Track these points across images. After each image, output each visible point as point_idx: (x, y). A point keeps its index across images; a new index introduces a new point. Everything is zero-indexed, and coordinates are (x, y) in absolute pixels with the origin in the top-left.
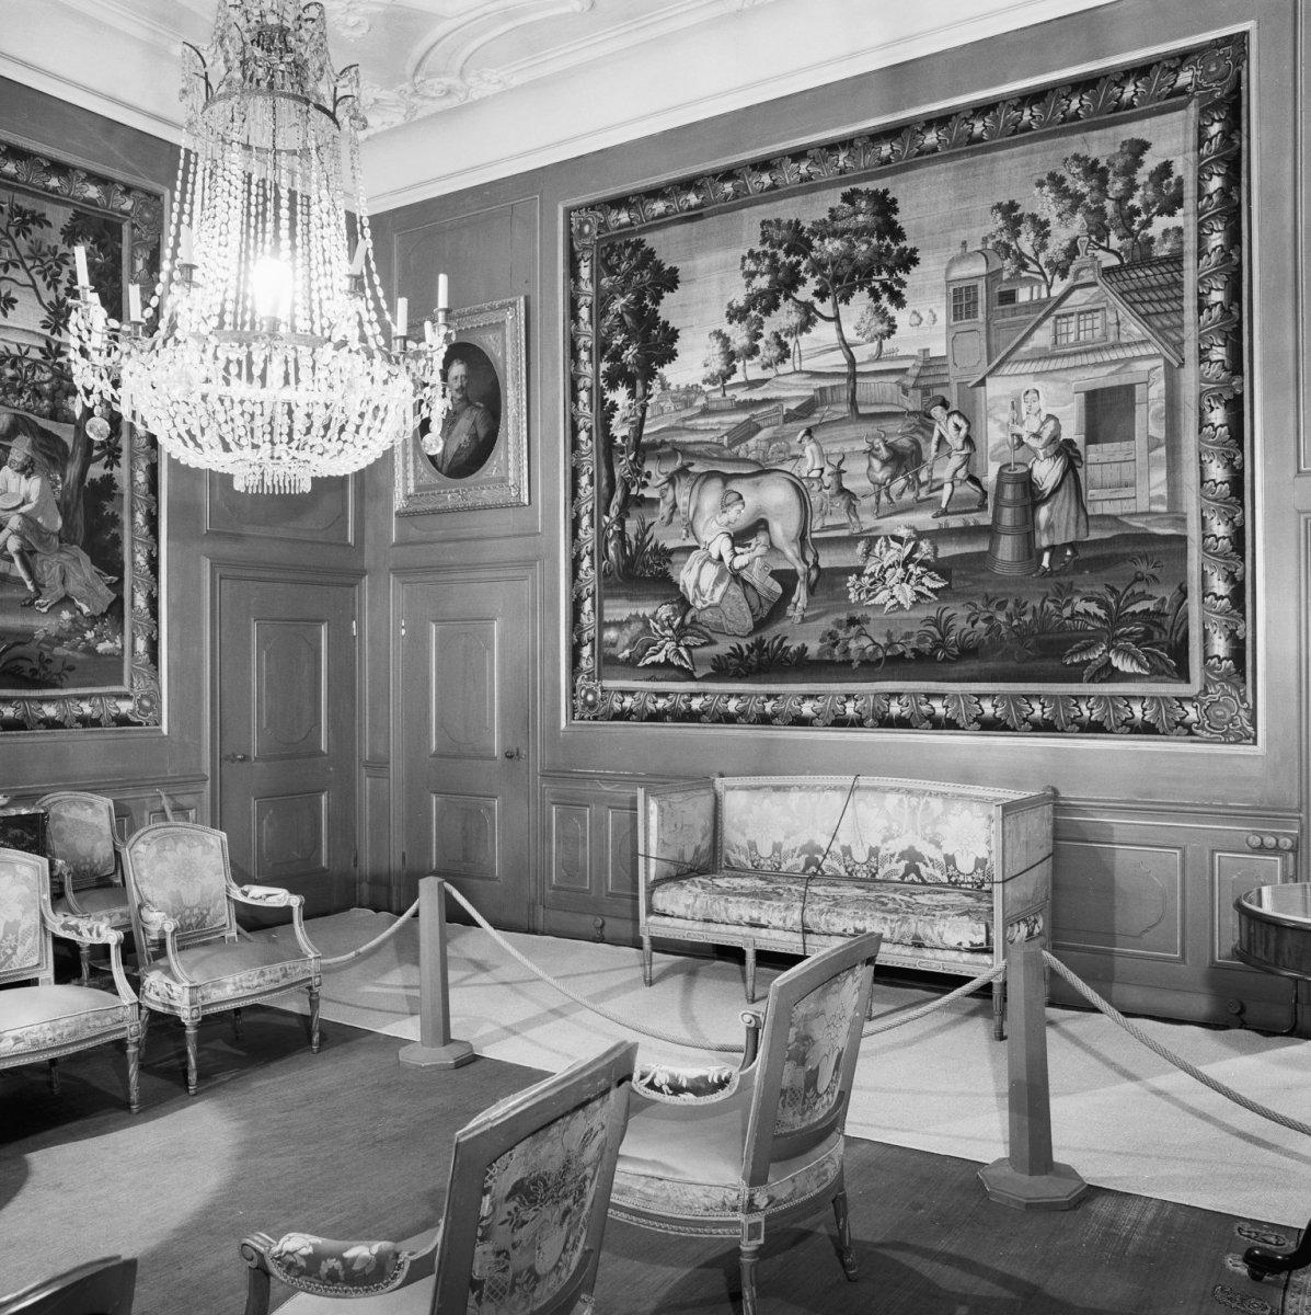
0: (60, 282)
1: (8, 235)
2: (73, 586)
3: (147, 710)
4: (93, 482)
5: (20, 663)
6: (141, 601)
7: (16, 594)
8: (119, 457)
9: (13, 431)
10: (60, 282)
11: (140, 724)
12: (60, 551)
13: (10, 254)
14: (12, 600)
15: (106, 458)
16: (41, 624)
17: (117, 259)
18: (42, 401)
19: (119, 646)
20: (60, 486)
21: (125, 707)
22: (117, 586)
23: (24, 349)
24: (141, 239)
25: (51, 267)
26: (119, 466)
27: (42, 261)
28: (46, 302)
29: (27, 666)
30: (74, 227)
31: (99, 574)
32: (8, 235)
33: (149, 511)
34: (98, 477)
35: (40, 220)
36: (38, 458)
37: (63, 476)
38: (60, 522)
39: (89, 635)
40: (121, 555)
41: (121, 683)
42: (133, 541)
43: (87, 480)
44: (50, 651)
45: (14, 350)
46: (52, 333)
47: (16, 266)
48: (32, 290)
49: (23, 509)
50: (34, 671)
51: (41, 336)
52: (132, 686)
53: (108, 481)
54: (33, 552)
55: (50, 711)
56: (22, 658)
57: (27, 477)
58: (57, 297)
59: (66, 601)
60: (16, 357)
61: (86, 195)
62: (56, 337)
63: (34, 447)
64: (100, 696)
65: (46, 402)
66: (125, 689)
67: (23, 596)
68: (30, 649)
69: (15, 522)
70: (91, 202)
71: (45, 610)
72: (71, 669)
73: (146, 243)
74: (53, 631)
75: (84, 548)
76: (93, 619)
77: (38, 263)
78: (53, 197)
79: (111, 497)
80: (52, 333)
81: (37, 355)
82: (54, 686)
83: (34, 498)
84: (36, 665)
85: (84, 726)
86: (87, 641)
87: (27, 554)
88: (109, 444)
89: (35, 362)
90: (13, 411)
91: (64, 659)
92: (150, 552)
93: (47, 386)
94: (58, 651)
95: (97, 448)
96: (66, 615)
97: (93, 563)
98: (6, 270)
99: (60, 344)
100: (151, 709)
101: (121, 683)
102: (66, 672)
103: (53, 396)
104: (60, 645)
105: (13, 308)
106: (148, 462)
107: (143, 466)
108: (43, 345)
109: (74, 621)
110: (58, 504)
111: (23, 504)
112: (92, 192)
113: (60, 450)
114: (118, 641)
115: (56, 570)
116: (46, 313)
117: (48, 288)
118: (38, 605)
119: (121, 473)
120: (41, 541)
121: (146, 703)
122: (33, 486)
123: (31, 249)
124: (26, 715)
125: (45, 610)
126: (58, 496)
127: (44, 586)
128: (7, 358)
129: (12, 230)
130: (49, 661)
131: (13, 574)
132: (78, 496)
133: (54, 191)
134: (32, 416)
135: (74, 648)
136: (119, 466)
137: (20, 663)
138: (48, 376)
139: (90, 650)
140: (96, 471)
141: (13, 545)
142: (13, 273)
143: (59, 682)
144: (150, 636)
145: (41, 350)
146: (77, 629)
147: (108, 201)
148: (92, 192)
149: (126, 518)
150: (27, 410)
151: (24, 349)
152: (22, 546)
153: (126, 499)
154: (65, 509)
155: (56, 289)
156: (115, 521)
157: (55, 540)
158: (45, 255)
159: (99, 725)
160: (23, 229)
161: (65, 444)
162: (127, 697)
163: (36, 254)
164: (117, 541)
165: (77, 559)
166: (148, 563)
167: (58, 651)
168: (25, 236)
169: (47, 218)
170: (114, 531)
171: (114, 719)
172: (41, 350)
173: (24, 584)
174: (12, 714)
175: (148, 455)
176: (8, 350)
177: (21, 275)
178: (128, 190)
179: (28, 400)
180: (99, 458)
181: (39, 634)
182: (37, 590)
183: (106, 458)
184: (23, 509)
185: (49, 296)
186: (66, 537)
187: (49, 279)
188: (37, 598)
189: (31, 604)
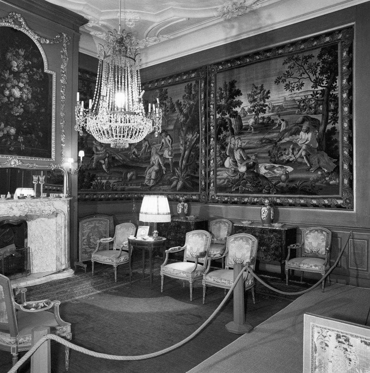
0: (317, 72)
1: (302, 66)
2: (322, 164)
3: (348, 203)
4: (328, 130)
5: (306, 187)
6: (346, 167)
7: (305, 167)
8: (338, 120)
9: (303, 122)
10: (317, 72)
11: (345, 208)
12: (318, 153)
13: (302, 71)
14: (303, 169)
15: (333, 122)
16: (311, 176)
17: (336, 57)
18: (311, 109)
19: (338, 182)
20: (317, 134)
21: (340, 202)
22: (337, 163)
23: (306, 96)
24: (345, 45)
25: (314, 69)
26: (338, 123)
27: (311, 69)
28: (312, 80)
29: (308, 189)
30: (321, 54)
31: (330, 159)
32: (302, 66)
33: (349, 136)
34: (330, 128)
35: (311, 57)
36: (312, 127)
37: (318, 131)
38: (317, 145)
39: (327, 179)
40: (339, 152)
41: (338, 194)
42: (343, 147)
43: (326, 130)
44: (315, 184)
45: (304, 98)
46: (315, 89)
47: (304, 73)
48: (309, 78)
49: (306, 143)
50: (310, 190)
51: (311, 91)
52: (342, 195)
53: (334, 129)
54: (309, 155)
55: (314, 202)
56: (306, 186)
57: (308, 133)
58: (316, 77)
59: (320, 168)
60: (304, 100)
61: (325, 41)
62: (316, 89)
63: (309, 124)
64: (331, 198)
65: (313, 110)
66: (340, 196)
67: (307, 168)
68: (308, 183)
69: (304, 147)
70: (328, 42)
71: (313, 172)
72: (321, 189)
73: (347, 45)
74: (315, 178)
75: (325, 152)
76: (328, 174)
77: (310, 70)
78: (315, 48)
79: (335, 134)
80: (315, 89)
81: (310, 97)
82: (316, 194)
83: (309, 139)
84: (310, 188)
85: (325, 207)
86: (327, 181)
87: (307, 156)
88: (334, 117)
89: (310, 100)
90: (303, 115)
91: (319, 186)
92: (349, 150)
93: (313, 105)
94: (317, 184)
95: (330, 119)
96: (319, 173)
97: (329, 155)
98: (301, 75)
99: (317, 91)
100: (350, 203)
101: (338, 194)
102: (319, 190)
103: (315, 108)
104: (318, 182)
105: (303, 86)
106: (348, 119)
107: (347, 121)
108: (312, 93)
109: (322, 174)
110: (317, 139)
111: (306, 141)
112: (328, 39)
113: (317, 123)
114: (337, 180)
115: (316, 159)
116: (313, 83)
117: (313, 76)
118: (311, 170)
119: (338, 126)
120: (311, 151)
121: (348, 201)
122: (310, 135)
123: (308, 67)
124: (307, 202)
125: (313, 172)
126: (317, 137)
127: (312, 164)
128: (302, 101)
129: (303, 64)
130: (314, 187)
131: (303, 162)
132: (323, 136)
133: (316, 45)
134: (309, 115)
135: (322, 183)
136: (338, 123)
137: (306, 187)
138: (314, 101)
139: (328, 183)
140: (329, 127)
141: (304, 153)
142: (304, 76)
143: (317, 193)
144: (349, 178)
145: (311, 95)
146: (323, 177)
147: (333, 39)
148: (328, 39)
149: (340, 139)
150: (307, 114)
151: (306, 96)
152: (306, 153)
153: (340, 133)
154: (319, 141)
155: (316, 75)
156: (336, 141)
157: (316, 151)
158: (312, 66)
159: (331, 207)
160: (306, 62)
161: (319, 121)
162: (340, 199)
163: (310, 68)
164: (337, 148)
165: (323, 155)
166: (349, 153)
167: (317, 184)
168: (306, 64)
169: (313, 55)
170: (336, 145)
171: (336, 206)
172: (311, 95)
173: (307, 164)
174: (303, 202)
175: (348, 117)
176: (302, 98)
177: (305, 76)
178: (340, 31)
179: (308, 111)
180: (330, 122)
181: (311, 179)
182: (311, 166)
183: (333, 122)
184: (306, 143)
185: (313, 78)
186: (320, 149)
187: (314, 73)
188: (311, 168)
189: (309, 170)
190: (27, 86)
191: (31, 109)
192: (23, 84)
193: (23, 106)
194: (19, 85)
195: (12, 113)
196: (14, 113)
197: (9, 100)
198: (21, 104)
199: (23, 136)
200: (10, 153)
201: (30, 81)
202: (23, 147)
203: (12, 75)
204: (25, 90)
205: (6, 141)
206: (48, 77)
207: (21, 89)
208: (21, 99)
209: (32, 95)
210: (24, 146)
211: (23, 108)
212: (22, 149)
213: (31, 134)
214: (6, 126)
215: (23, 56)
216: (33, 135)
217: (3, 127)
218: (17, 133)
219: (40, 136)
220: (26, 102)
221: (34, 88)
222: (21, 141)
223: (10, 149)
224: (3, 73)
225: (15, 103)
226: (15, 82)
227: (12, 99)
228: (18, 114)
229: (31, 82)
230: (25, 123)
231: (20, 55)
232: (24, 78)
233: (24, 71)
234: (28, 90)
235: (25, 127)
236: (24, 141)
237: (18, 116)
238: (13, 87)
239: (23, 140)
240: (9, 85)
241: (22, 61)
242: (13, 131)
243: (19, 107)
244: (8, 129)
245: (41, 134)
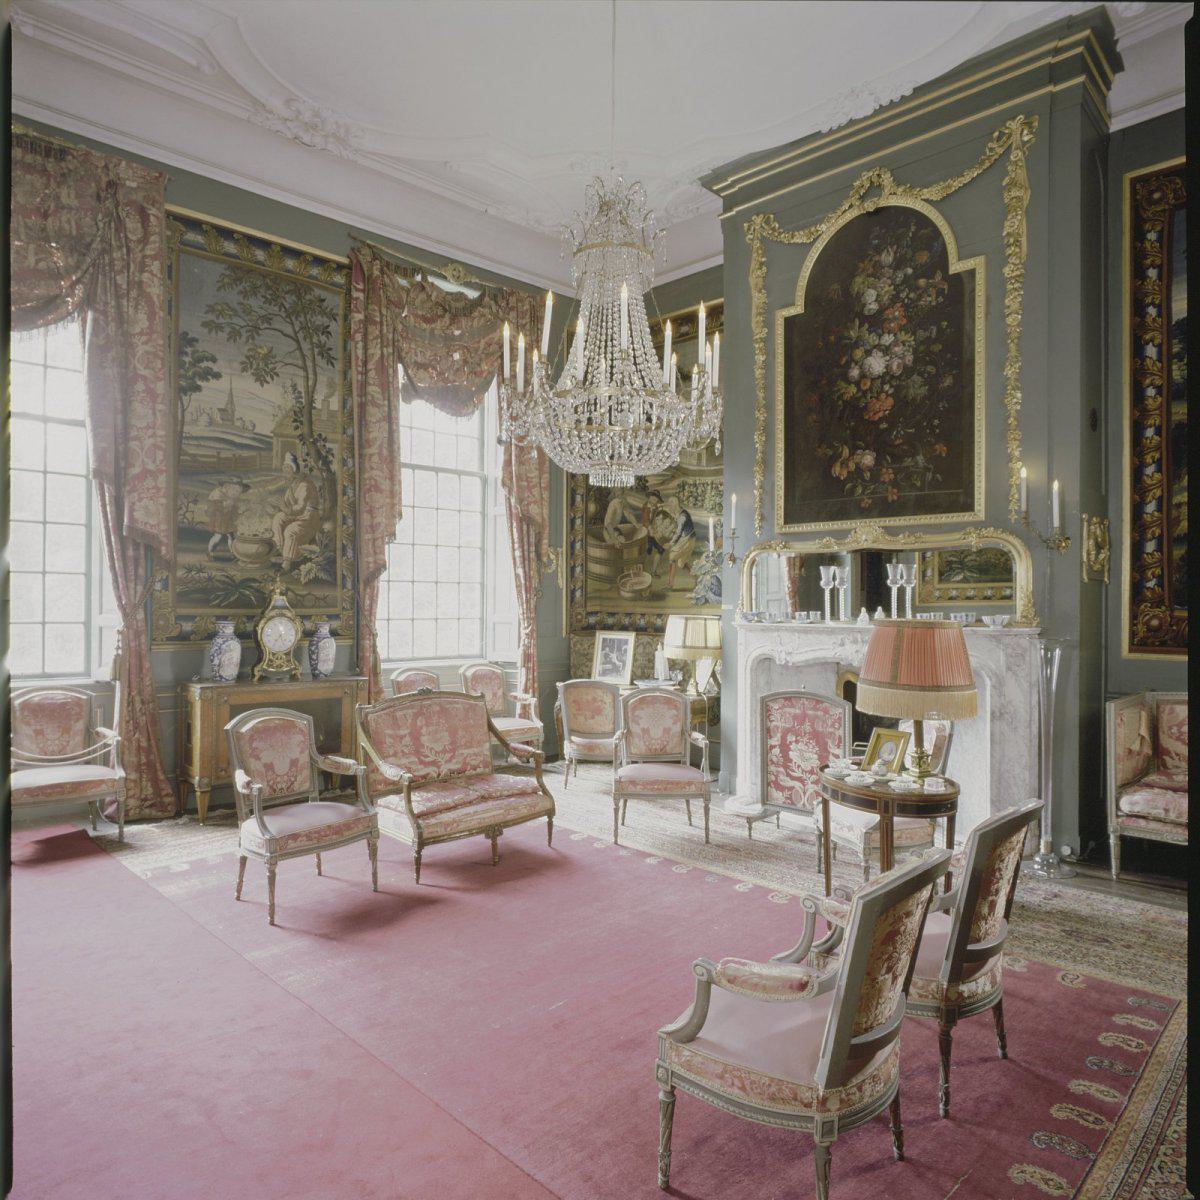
190: (903, 336)
191: (911, 391)
192: (892, 335)
193: (890, 392)
194: (883, 342)
195: (867, 417)
196: (872, 414)
197: (859, 389)
198: (887, 387)
199: (894, 466)
200: (864, 513)
201: (910, 319)
202: (892, 496)
203: (867, 326)
204: (896, 349)
205: (854, 487)
206: (960, 286)
207: (886, 350)
208: (887, 376)
209: (915, 352)
210: (895, 491)
211: (891, 395)
212: (890, 499)
213: (913, 455)
214: (852, 454)
215: (890, 267)
216: (920, 459)
217: (848, 455)
218: (878, 461)
219: (940, 456)
220: (899, 378)
221: (921, 334)
222: (887, 480)
223: (863, 505)
224: (846, 334)
225: (871, 392)
226: (873, 339)
227: (865, 384)
228: (881, 414)
229: (916, 320)
230: (898, 432)
231: (883, 268)
232: (895, 318)
233: (895, 299)
234: (904, 345)
235: (898, 442)
236: (895, 478)
237: (881, 420)
238: (868, 353)
239: (892, 475)
240: (859, 353)
241: (888, 278)
242: (868, 459)
243: (883, 396)
244: (857, 458)
245: (941, 449)
